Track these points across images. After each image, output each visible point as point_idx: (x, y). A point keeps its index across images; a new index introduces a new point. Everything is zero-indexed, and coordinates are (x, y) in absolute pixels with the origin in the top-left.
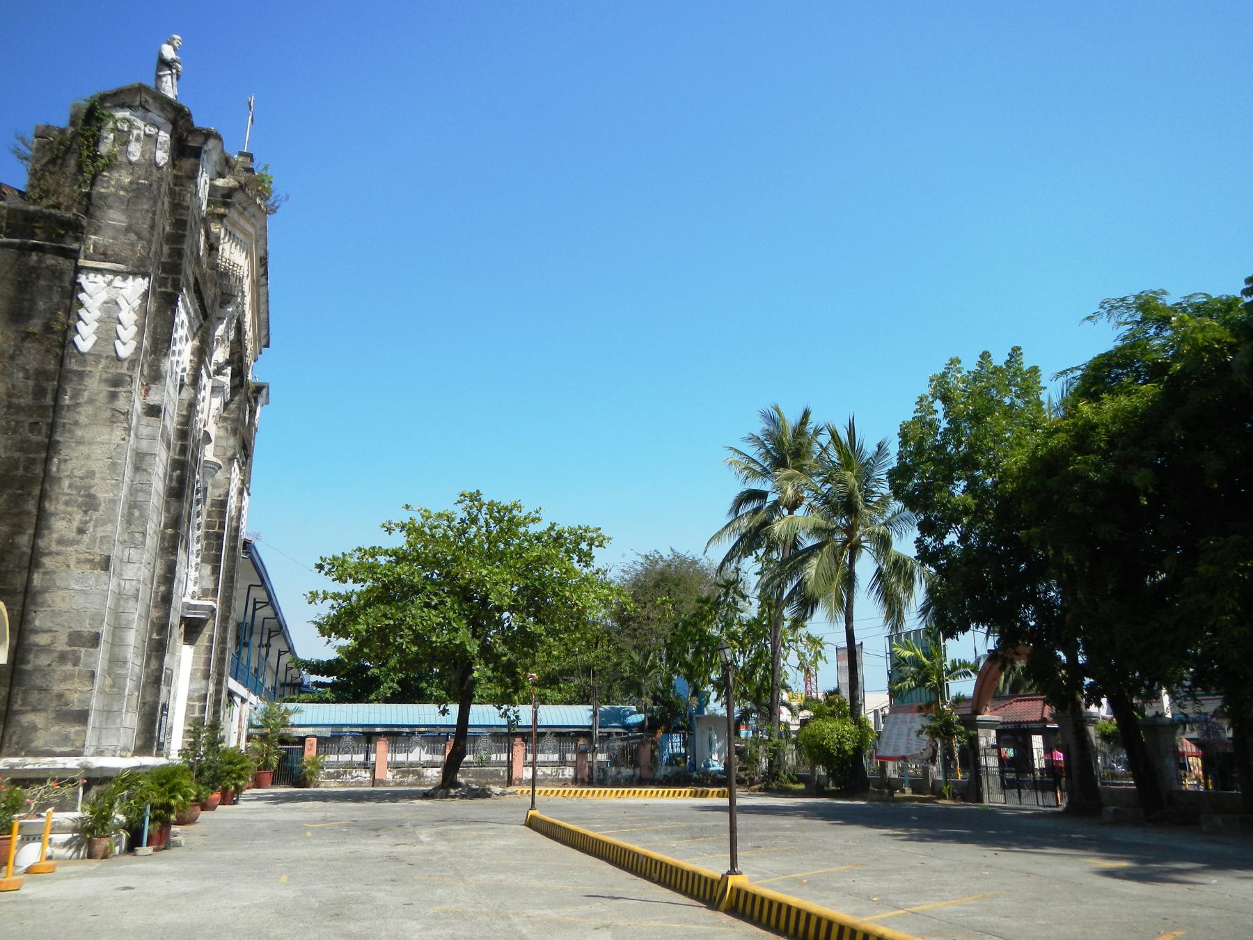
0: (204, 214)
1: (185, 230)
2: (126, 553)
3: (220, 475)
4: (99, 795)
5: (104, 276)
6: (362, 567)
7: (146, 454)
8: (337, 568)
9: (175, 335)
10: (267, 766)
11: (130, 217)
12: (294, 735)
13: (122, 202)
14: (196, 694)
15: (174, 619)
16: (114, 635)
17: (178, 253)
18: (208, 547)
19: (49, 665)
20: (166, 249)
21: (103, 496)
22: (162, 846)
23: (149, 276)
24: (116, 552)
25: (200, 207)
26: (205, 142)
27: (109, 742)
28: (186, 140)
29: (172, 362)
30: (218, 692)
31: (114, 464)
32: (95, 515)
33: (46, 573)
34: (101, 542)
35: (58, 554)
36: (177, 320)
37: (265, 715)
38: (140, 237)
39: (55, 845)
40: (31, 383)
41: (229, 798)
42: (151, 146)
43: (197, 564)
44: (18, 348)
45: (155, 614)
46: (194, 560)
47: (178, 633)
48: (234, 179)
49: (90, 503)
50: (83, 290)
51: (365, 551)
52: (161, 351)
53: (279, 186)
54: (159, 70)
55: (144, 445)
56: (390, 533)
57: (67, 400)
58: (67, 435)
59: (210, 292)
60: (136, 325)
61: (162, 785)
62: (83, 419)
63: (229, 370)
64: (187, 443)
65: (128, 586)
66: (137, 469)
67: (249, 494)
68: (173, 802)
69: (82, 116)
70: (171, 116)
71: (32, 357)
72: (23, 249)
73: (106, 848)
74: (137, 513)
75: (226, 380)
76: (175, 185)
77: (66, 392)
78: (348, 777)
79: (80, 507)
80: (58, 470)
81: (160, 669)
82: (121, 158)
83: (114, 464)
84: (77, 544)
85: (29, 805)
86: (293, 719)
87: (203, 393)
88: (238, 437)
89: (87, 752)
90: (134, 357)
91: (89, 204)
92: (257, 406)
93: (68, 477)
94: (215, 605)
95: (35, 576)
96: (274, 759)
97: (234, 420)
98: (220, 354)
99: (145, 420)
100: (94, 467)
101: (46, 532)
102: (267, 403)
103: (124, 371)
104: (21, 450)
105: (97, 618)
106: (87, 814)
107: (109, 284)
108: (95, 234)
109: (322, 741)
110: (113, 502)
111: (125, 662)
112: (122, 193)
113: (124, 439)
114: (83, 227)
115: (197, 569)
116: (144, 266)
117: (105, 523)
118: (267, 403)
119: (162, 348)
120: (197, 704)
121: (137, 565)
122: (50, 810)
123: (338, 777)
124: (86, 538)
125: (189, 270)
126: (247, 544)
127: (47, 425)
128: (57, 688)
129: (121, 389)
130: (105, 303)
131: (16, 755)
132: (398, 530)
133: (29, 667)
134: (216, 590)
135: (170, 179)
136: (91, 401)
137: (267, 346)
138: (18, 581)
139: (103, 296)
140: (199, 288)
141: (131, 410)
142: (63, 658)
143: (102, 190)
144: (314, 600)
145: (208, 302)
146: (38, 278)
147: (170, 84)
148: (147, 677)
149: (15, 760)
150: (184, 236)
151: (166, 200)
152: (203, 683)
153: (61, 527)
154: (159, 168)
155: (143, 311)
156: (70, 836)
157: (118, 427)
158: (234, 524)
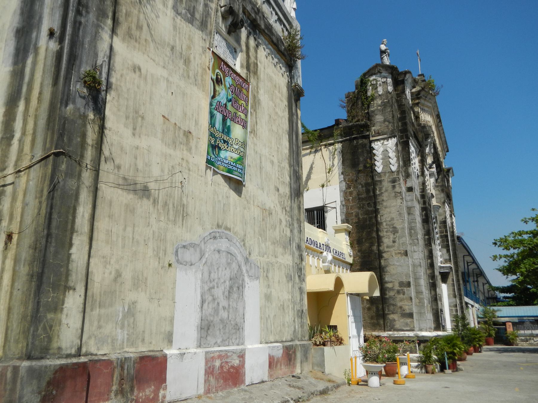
0: (411, 105)
1: (405, 114)
3: (441, 210)
4: (425, 347)
5: (380, 141)
6: (517, 242)
7: (411, 207)
8: (503, 243)
9: (411, 157)
10: (490, 335)
11: (384, 116)
12: (500, 321)
13: (380, 111)
14: (452, 304)
15: (437, 273)
16: (415, 282)
17: (405, 124)
18: (443, 241)
19: (394, 295)
20: (400, 124)
21: (399, 226)
22: (455, 370)
23: (396, 136)
24: (409, 249)
25: (409, 103)
26: (405, 76)
27: (423, 325)
28: (398, 78)
29: (412, 168)
30: (461, 303)
31: (400, 214)
32: (398, 235)
33: (385, 260)
34: (403, 245)
35: (388, 252)
36: (411, 151)
37: (484, 313)
38: (390, 123)
39: (412, 367)
40: (364, 189)
41: (477, 350)
42: (385, 86)
43: (440, 249)
44: (357, 177)
45: (429, 272)
46: (439, 248)
47: (439, 278)
48: (419, 87)
49: (395, 231)
50: (374, 149)
51: (516, 233)
52: (407, 165)
53: (437, 82)
54: (381, 56)
55: (410, 204)
56: (527, 223)
57: (378, 192)
58: (381, 205)
59: (420, 136)
61: (449, 344)
62: (385, 198)
63: (434, 166)
64: (425, 200)
66: (409, 214)
67: (455, 216)
68: (455, 351)
69: (359, 84)
70: (390, 71)
71: (363, 179)
72: (351, 140)
73: (432, 370)
74: (413, 232)
75: (434, 170)
76: (397, 98)
78: (532, 341)
79: (391, 232)
81: (436, 295)
82: (376, 95)
83: (400, 214)
85: (399, 351)
86: (498, 314)
87: (427, 177)
89: (416, 329)
90: (398, 170)
91: (369, 116)
92: (449, 178)
93: (385, 221)
94: (451, 266)
95: (382, 261)
96: (493, 333)
97: (441, 186)
98: (430, 160)
99: (408, 194)
100: (393, 216)
101: (382, 244)
102: (453, 175)
103: (395, 176)
104: (366, 214)
105: (407, 275)
106: (422, 355)
107: (383, 144)
108: (373, 127)
109: (514, 324)
110: (403, 228)
111: (422, 293)
112: (379, 108)
113: (402, 203)
114: (369, 126)
115: (440, 251)
116: (393, 133)
117: (402, 238)
118: (453, 175)
120: (453, 308)
121: (418, 253)
122: (408, 353)
123: (527, 341)
124: (396, 244)
125: (410, 129)
126: (459, 238)
128: (399, 304)
129: (396, 183)
130: (383, 151)
131: (390, 331)
132: (530, 221)
133: (387, 296)
134: (450, 259)
135: (395, 96)
136: (386, 191)
137: (448, 151)
138: (376, 264)
139: (382, 149)
140: (416, 135)
142: (398, 292)
143: (372, 109)
144: (495, 259)
145: (420, 140)
146: (358, 149)
147: (386, 59)
148: (432, 298)
149: (390, 333)
150: (405, 117)
151: (396, 105)
152: (454, 299)
153: (387, 241)
154: (390, 93)
155: (397, 151)
156: (416, 364)
158: (451, 230)
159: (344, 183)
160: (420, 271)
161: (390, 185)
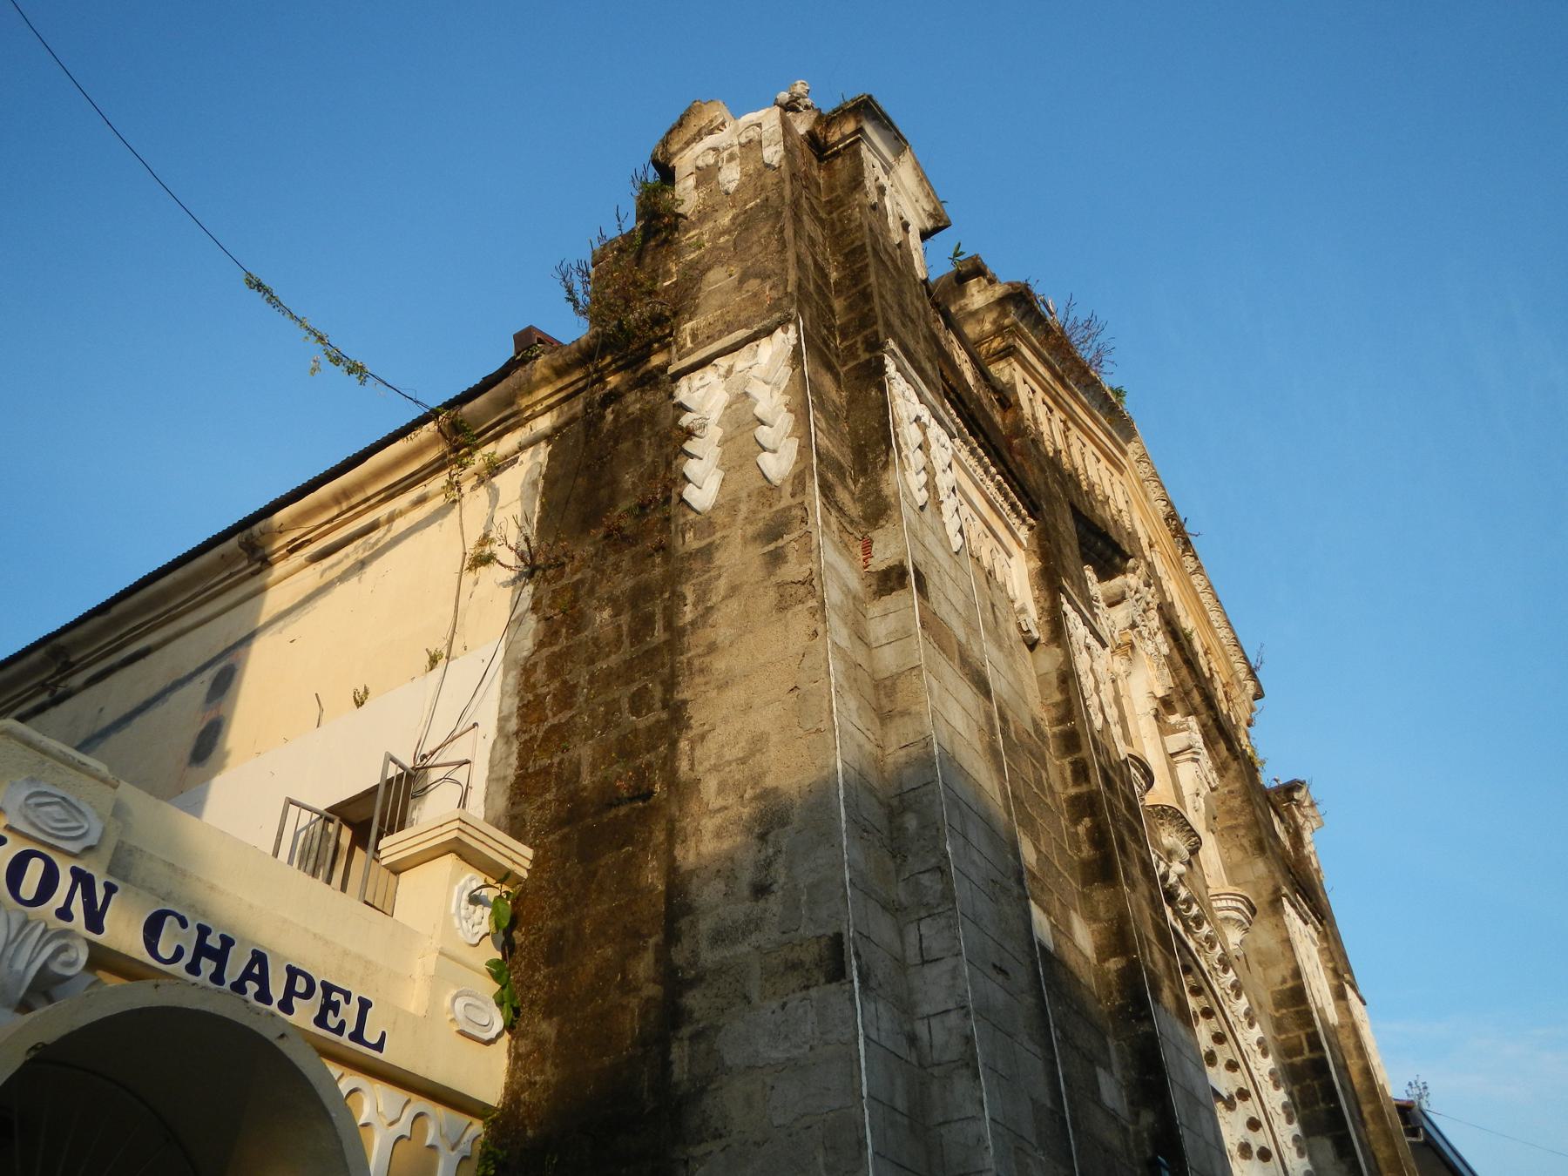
2: (912, 938)
7: (895, 678)
33: (696, 1037)
43: (1296, 1139)
55: (888, 660)
57: (688, 613)
60: (790, 411)
64: (1084, 754)
65: (939, 1037)
74: (911, 822)
77: (685, 598)
80: (692, 769)
84: (758, 928)
88: (1269, 853)
90: (801, 466)
93: (716, 768)
103: (786, 501)
119: (878, 456)
121: (949, 963)
124: (774, 904)
127: (663, 683)
136: (734, 590)
137: (1259, 695)
141: (815, 567)
157: (795, 615)
159: (531, 622)
160: (970, 1110)
161: (758, 551)
